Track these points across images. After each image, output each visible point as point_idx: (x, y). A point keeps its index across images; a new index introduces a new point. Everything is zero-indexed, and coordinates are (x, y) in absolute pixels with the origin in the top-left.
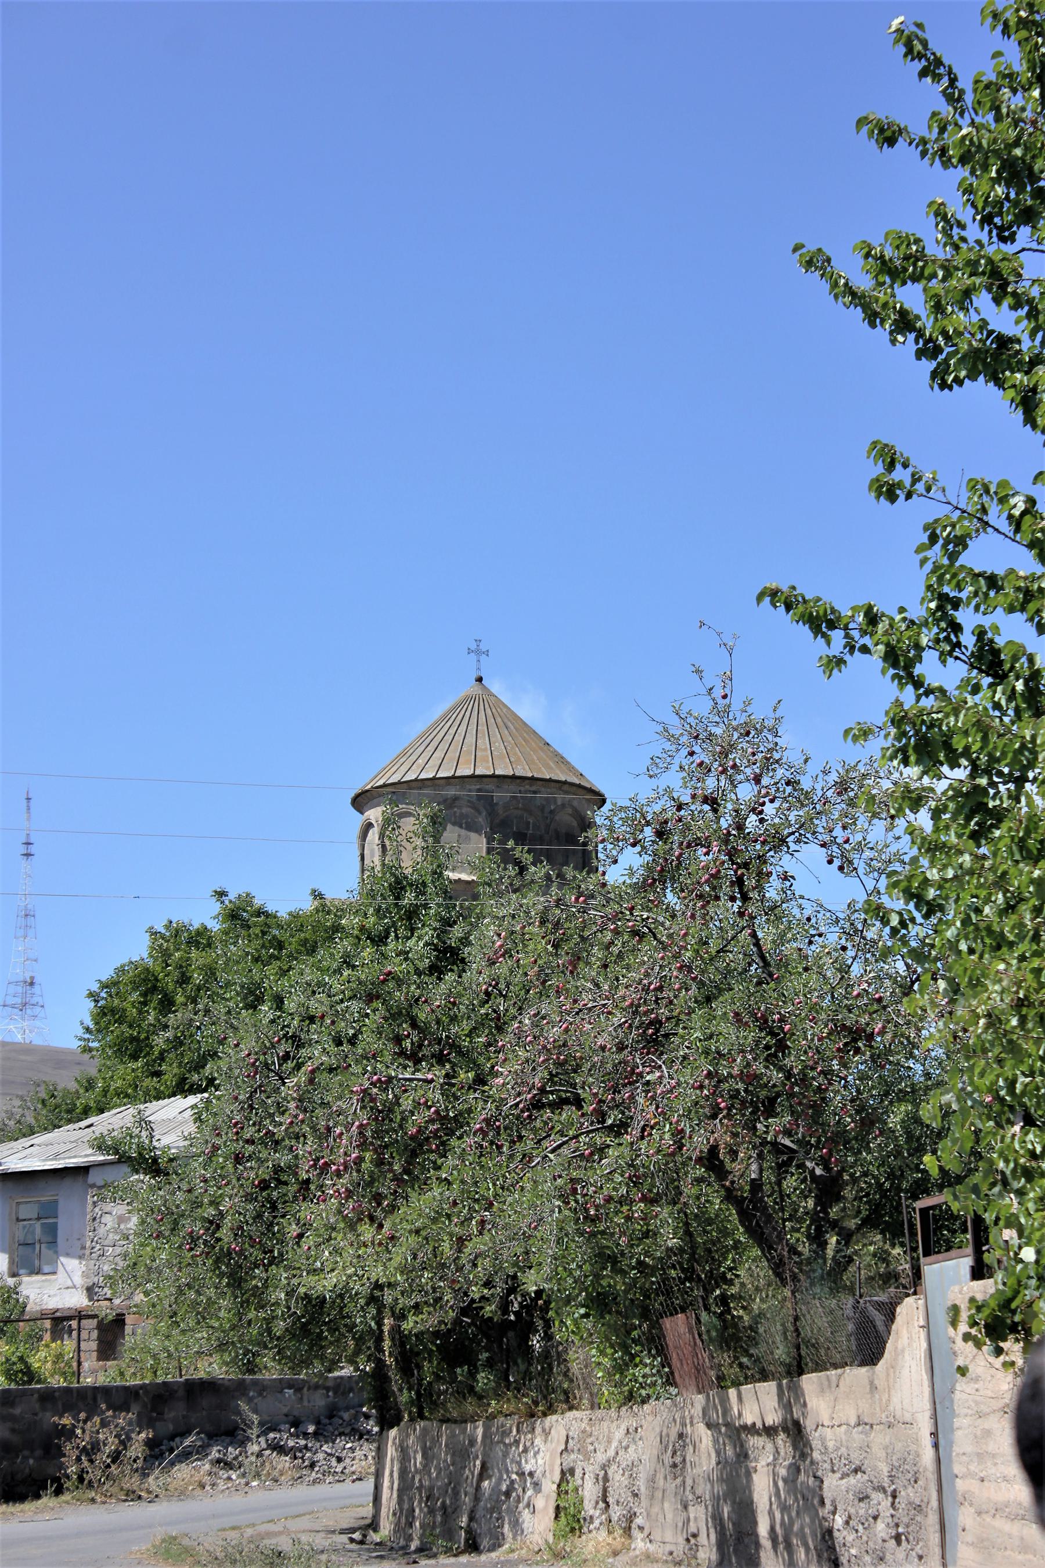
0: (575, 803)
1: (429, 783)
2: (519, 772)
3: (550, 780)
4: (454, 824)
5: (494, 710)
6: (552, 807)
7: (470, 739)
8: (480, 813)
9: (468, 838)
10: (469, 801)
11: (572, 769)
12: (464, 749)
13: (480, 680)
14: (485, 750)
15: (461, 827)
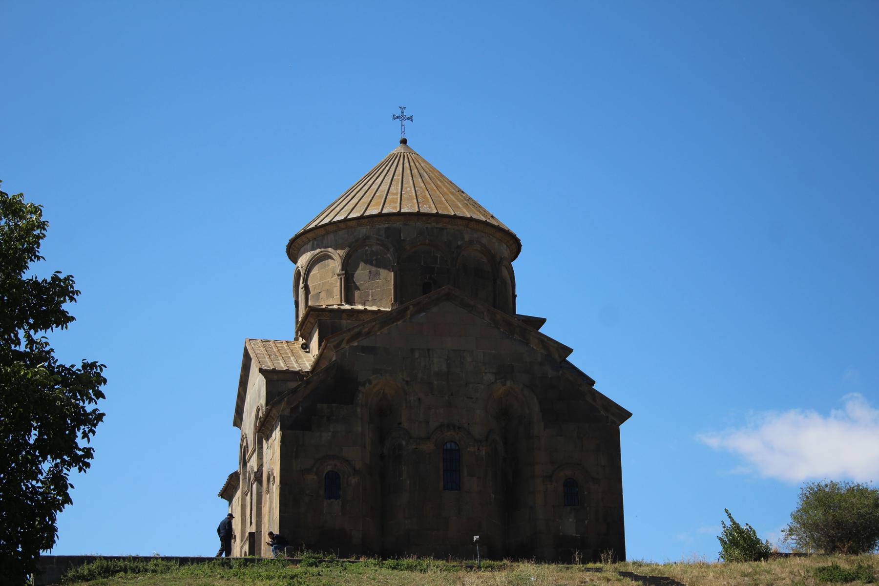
0: (484, 241)
1: (342, 225)
2: (425, 209)
3: (455, 217)
4: (366, 262)
5: (412, 164)
6: (459, 243)
7: (384, 187)
8: (388, 250)
9: (378, 274)
10: (378, 239)
11: (485, 212)
12: (377, 194)
13: (404, 142)
14: (397, 194)
15: (371, 264)
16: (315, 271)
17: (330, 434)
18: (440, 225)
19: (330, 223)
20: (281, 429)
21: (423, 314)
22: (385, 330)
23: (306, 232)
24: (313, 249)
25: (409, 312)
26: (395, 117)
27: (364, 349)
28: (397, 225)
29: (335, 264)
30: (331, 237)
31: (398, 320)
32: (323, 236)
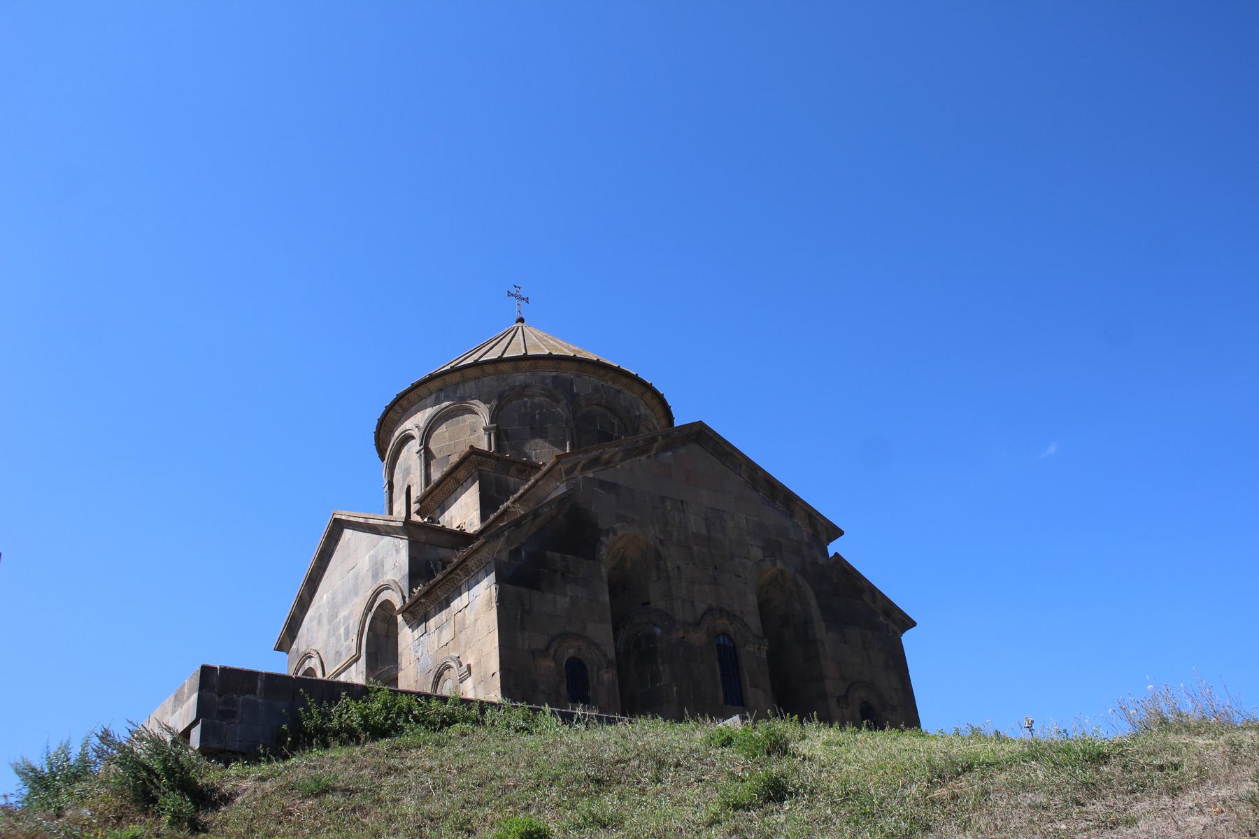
1: (489, 369)
2: (603, 360)
16: (442, 430)
17: (567, 599)
18: (616, 387)
19: (476, 364)
20: (499, 580)
21: (669, 454)
22: (627, 463)
23: (432, 378)
24: (437, 402)
25: (656, 445)
26: (510, 294)
27: (603, 484)
28: (567, 375)
29: (481, 416)
30: (471, 385)
31: (641, 453)
32: (457, 385)
